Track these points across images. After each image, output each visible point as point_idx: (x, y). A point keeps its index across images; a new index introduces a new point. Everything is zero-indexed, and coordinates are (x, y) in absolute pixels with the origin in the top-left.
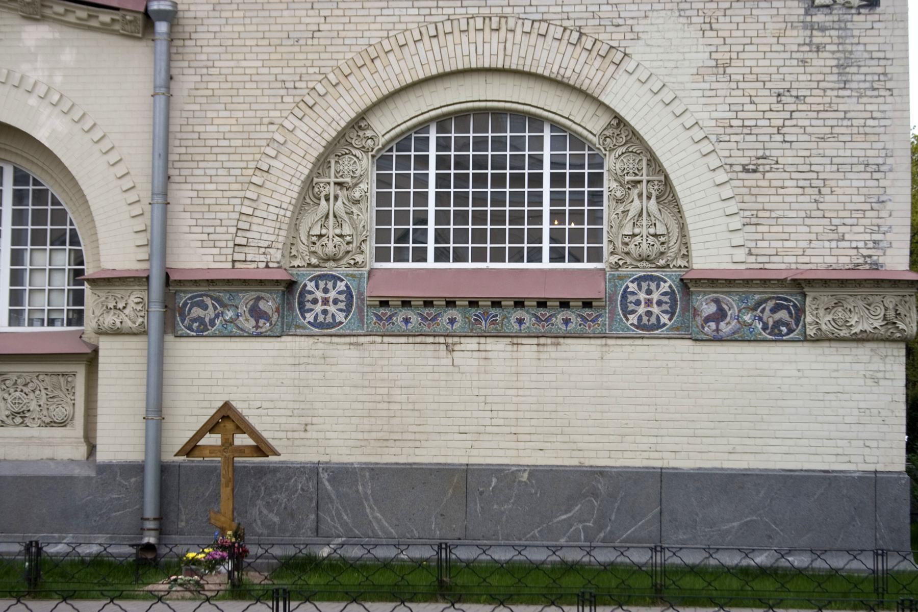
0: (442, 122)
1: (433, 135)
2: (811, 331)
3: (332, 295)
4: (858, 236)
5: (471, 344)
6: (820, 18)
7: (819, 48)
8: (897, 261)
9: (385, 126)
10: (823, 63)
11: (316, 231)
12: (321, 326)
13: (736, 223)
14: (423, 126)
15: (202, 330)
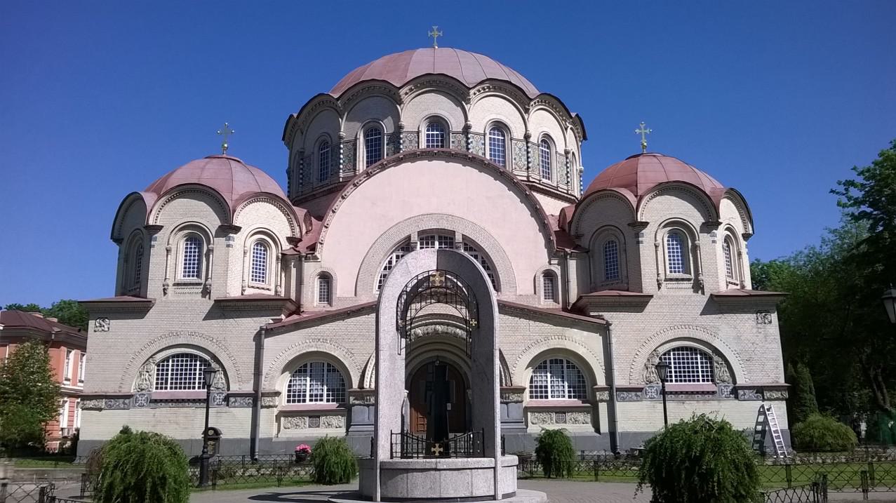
0: (674, 350)
1: (672, 353)
2: (766, 397)
3: (653, 391)
4: (773, 376)
5: (688, 402)
6: (759, 326)
7: (760, 333)
8: (782, 381)
9: (662, 350)
10: (761, 336)
11: (648, 376)
12: (651, 398)
13: (746, 373)
14: (670, 351)
15: (624, 400)
